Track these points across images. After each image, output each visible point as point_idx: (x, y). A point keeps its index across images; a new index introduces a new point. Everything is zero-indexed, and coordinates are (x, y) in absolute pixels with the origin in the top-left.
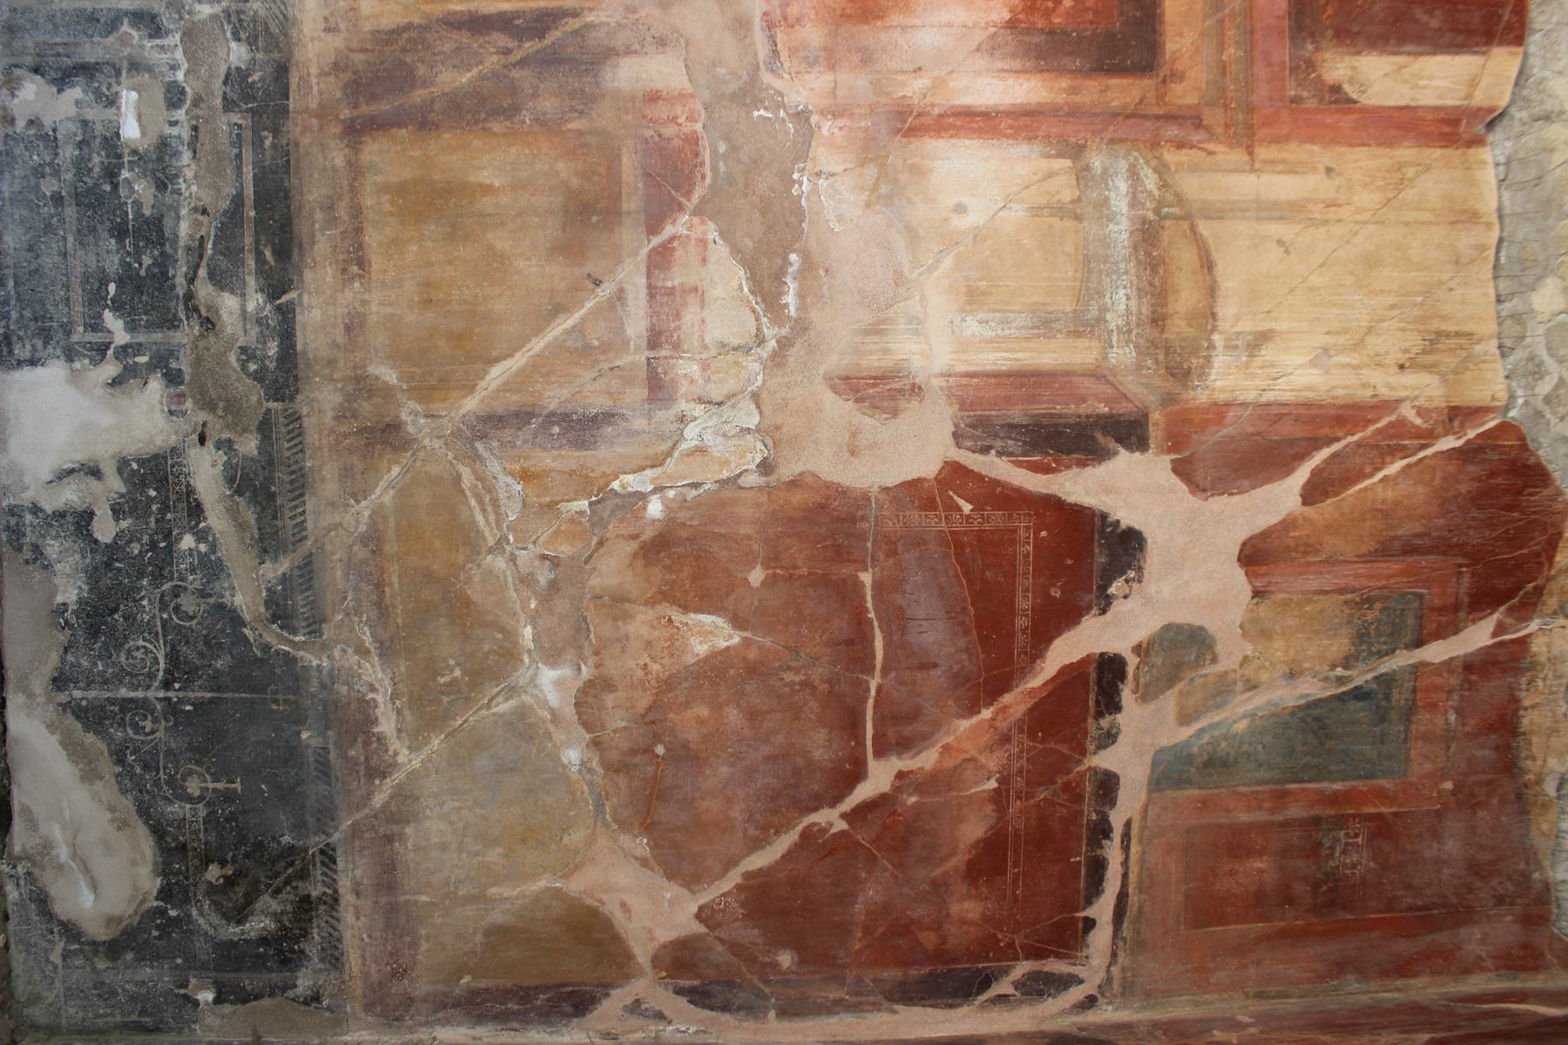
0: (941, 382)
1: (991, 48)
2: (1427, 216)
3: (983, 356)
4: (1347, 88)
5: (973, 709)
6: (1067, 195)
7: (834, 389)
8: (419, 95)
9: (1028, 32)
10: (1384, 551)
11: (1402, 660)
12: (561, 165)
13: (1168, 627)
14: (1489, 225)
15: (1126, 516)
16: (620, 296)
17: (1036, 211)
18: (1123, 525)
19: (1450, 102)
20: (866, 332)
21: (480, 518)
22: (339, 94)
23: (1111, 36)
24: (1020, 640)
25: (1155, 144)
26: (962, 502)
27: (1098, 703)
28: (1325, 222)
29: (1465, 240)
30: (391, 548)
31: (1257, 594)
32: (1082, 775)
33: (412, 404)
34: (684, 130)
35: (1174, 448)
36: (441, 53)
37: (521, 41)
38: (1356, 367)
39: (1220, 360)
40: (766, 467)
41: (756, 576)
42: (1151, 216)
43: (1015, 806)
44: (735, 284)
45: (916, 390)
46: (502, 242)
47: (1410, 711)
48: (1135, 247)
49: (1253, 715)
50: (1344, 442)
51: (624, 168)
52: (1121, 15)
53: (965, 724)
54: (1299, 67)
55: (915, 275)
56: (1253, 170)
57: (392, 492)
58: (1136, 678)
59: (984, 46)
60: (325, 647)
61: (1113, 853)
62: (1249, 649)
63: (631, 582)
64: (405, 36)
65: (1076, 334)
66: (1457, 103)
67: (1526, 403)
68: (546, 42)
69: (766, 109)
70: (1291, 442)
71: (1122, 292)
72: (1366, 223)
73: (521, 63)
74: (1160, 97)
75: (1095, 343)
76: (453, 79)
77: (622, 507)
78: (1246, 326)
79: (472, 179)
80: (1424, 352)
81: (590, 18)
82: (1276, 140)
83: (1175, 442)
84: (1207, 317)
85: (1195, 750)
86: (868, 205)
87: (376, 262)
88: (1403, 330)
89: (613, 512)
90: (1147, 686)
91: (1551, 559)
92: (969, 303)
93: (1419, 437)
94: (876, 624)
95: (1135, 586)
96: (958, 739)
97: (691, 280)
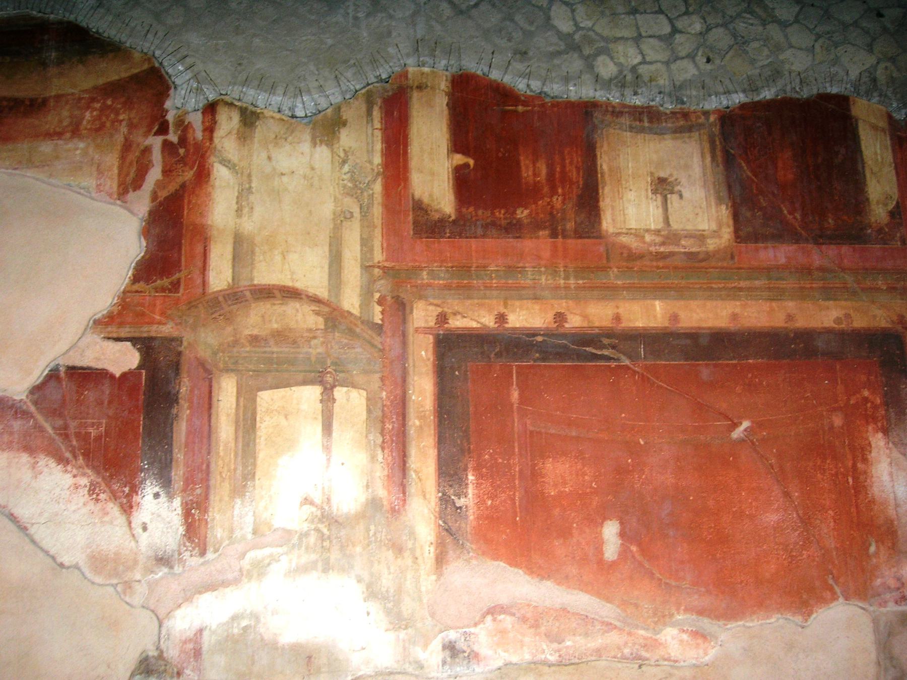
4: (890, 207)
9: (888, 420)
19: (889, 142)
54: (882, 238)
59: (902, 450)
66: (888, 138)
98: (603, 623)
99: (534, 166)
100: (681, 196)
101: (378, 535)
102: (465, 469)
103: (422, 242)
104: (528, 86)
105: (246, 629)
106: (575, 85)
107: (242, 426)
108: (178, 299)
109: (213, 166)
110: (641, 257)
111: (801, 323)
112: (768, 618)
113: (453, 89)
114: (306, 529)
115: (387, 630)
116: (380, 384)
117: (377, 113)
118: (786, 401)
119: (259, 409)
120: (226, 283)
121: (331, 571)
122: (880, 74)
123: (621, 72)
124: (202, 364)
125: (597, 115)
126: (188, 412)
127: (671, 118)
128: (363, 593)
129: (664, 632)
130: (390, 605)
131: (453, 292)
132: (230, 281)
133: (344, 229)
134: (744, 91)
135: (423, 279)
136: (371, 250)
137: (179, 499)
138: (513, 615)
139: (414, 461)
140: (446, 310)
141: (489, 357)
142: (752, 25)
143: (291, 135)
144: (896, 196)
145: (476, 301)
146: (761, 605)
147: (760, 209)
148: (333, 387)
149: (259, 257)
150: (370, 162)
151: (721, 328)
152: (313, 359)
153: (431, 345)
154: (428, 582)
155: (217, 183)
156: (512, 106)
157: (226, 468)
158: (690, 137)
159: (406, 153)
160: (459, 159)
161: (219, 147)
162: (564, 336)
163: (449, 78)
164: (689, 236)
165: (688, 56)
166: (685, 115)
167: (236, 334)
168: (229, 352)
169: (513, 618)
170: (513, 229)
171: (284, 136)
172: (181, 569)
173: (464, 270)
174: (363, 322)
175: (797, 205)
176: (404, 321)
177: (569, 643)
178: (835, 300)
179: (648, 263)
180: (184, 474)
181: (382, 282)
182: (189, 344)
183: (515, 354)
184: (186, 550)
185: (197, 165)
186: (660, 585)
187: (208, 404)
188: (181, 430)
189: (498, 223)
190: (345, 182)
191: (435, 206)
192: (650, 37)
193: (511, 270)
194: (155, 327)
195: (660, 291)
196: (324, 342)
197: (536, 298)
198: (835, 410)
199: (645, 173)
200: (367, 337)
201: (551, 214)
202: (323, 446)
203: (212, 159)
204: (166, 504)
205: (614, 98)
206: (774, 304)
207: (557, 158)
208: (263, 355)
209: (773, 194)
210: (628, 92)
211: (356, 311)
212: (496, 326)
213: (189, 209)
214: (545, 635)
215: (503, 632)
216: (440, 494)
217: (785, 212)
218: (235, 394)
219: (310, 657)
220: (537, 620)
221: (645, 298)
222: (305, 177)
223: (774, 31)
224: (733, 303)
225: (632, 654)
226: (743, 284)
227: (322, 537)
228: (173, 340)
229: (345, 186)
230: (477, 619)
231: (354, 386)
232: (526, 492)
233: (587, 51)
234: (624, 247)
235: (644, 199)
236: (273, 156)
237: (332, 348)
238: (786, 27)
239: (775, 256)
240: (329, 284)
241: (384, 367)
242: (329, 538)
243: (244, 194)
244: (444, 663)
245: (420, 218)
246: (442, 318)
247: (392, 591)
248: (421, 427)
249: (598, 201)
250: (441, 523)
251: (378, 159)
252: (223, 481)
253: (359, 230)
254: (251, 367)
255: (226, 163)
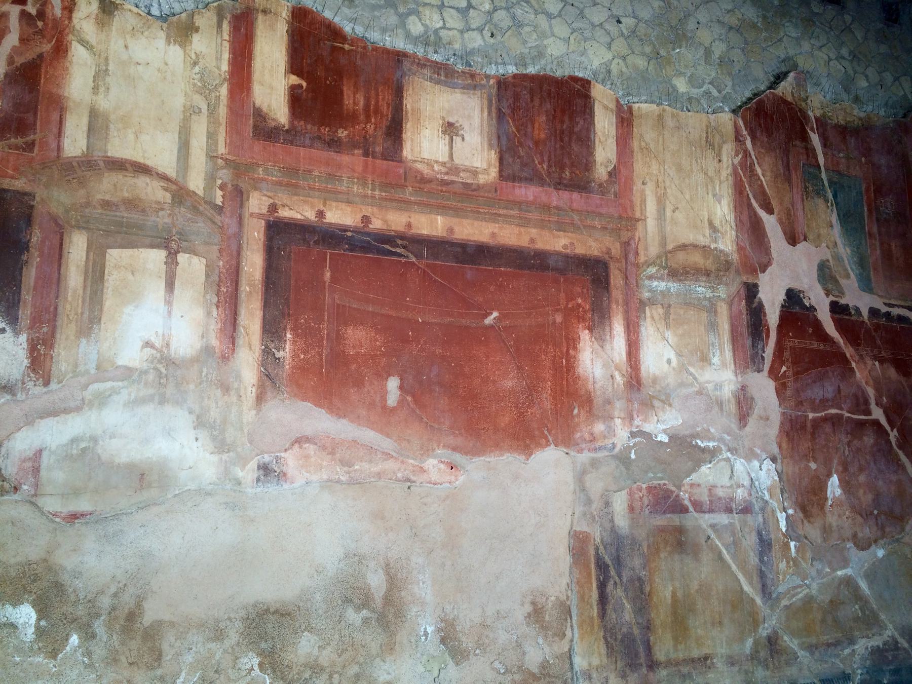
0: (739, 376)
1: (601, 340)
2: (661, 140)
3: (727, 356)
5: (852, 370)
6: (661, 311)
7: (745, 426)
8: (636, 631)
9: (593, 321)
10: (788, 179)
11: (824, 176)
12: (662, 555)
13: (819, 281)
14: (664, 110)
15: (782, 297)
16: (713, 526)
17: (668, 326)
18: (785, 298)
20: (721, 409)
21: (800, 596)
22: (636, 675)
23: (593, 281)
24: (828, 348)
25: (637, 266)
26: (782, 371)
27: (846, 315)
28: (665, 188)
29: (670, 123)
30: (814, 640)
31: (805, 239)
32: (871, 323)
33: (760, 630)
34: (645, 493)
35: (756, 271)
36: (616, 620)
37: (610, 577)
38: (720, 181)
39: (721, 246)
40: (774, 460)
41: (813, 466)
42: (666, 271)
43: (884, 354)
44: (708, 471)
45: (743, 388)
46: (695, 586)
47: (839, 173)
48: (680, 280)
49: (844, 245)
50: (749, 192)
51: (662, 524)
52: (583, 276)
53: (858, 374)
55: (697, 385)
56: (645, 220)
57: (793, 640)
58: (837, 297)
59: (601, 344)
60: (854, 672)
61: (896, 311)
62: (824, 245)
63: (818, 523)
64: (609, 639)
65: (716, 312)
67: (722, 102)
68: (610, 563)
69: (630, 453)
70: (750, 217)
71: (698, 289)
72: (664, 169)
73: (620, 577)
74: (618, 261)
75: (719, 304)
76: (628, 615)
77: (793, 529)
78: (707, 232)
79: (669, 601)
80: (714, 149)
81: (598, 540)
82: (632, 207)
83: (753, 271)
84: (704, 250)
85: (858, 272)
86: (670, 405)
87: (706, 651)
88: (705, 158)
89: (795, 532)
90: (839, 292)
91: (790, 104)
92: (707, 361)
93: (746, 157)
94: (826, 412)
95: (805, 294)
96: (863, 378)
97: (706, 492)
98: (383, 453)
99: (354, 97)
100: (463, 139)
101: (210, 376)
102: (285, 329)
103: (260, 144)
104: (353, 29)
105: (84, 450)
106: (390, 36)
107: (90, 277)
108: (33, 158)
109: (71, 43)
110: (430, 181)
111: (540, 245)
112: (502, 455)
113: (293, 19)
114: (145, 368)
115: (212, 453)
116: (218, 255)
117: (226, 26)
118: (524, 301)
119: (107, 263)
120: (80, 151)
121: (166, 404)
122: (614, 68)
123: (426, 32)
124: (54, 219)
125: (406, 64)
126: (38, 259)
127: (462, 76)
128: (194, 422)
129: (428, 462)
130: (215, 433)
131: (283, 188)
132: (85, 150)
133: (192, 121)
134: (516, 65)
135: (259, 174)
136: (216, 143)
137: (25, 335)
138: (316, 444)
139: (243, 319)
140: (277, 201)
141: (308, 243)
142: (527, 12)
143: (147, 30)
144: (614, 161)
145: (301, 198)
146: (497, 446)
147: (519, 157)
148: (177, 252)
149: (113, 132)
150: (219, 68)
151: (483, 243)
152: (160, 227)
153: (263, 229)
154: (249, 415)
155: (75, 59)
156: (340, 43)
157: (73, 312)
158: (474, 94)
159: (250, 66)
160: (294, 80)
161: (78, 27)
162: (368, 234)
163: (290, 9)
164: (466, 170)
165: (477, 29)
166: (473, 76)
167: (88, 197)
168: (81, 212)
169: (316, 447)
170: (334, 144)
171: (141, 30)
172: (24, 397)
173: (292, 171)
174: (206, 202)
175: (546, 159)
176: (241, 206)
177: (357, 467)
178: (565, 231)
179: (435, 187)
180: (31, 314)
181: (224, 171)
182: (42, 199)
183: (330, 243)
184: (31, 380)
185: (55, 39)
186: (426, 427)
187: (58, 254)
188: (30, 275)
189: (323, 138)
190: (196, 81)
191: (272, 115)
192: (451, 7)
193: (331, 177)
194: (7, 180)
195: (442, 209)
196: (170, 215)
197: (349, 202)
198: (557, 310)
199: (439, 117)
200: (209, 214)
201: (365, 137)
202: (165, 300)
203: (71, 37)
204: (11, 339)
205: (420, 52)
206: (522, 229)
207: (373, 93)
208: (115, 219)
209: (529, 147)
210: (431, 50)
211: (200, 192)
212: (316, 219)
213: (46, 79)
214: (339, 460)
215: (307, 457)
216: (263, 347)
217: (537, 162)
218: (85, 248)
219: (142, 475)
220: (334, 449)
221: (430, 213)
222: (159, 70)
223: (542, 21)
224: (493, 224)
225: (403, 477)
226: (502, 212)
227: (160, 375)
228: (25, 194)
229: (195, 85)
230: (287, 446)
231: (195, 254)
232: (331, 350)
233: (402, 9)
234: (417, 171)
235: (436, 137)
236: (130, 45)
237: (177, 220)
238: (551, 19)
239: (526, 194)
240: (177, 166)
241: (222, 241)
242: (166, 376)
243: (100, 76)
244: (258, 480)
245: (259, 123)
246: (273, 208)
247: (218, 422)
248: (251, 292)
249: (401, 133)
250: (262, 369)
251: (225, 67)
252: (70, 323)
253: (205, 125)
254: (101, 227)
255: (84, 43)
